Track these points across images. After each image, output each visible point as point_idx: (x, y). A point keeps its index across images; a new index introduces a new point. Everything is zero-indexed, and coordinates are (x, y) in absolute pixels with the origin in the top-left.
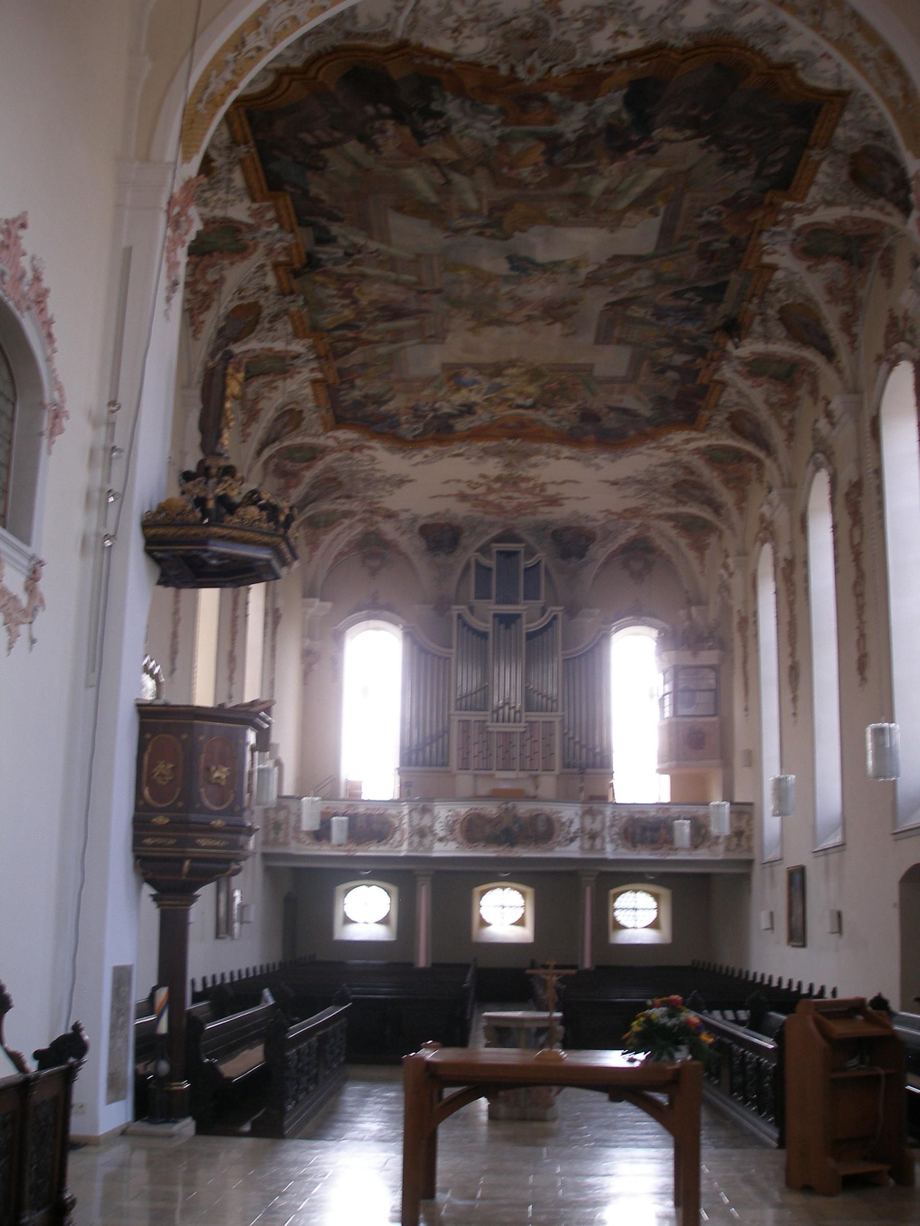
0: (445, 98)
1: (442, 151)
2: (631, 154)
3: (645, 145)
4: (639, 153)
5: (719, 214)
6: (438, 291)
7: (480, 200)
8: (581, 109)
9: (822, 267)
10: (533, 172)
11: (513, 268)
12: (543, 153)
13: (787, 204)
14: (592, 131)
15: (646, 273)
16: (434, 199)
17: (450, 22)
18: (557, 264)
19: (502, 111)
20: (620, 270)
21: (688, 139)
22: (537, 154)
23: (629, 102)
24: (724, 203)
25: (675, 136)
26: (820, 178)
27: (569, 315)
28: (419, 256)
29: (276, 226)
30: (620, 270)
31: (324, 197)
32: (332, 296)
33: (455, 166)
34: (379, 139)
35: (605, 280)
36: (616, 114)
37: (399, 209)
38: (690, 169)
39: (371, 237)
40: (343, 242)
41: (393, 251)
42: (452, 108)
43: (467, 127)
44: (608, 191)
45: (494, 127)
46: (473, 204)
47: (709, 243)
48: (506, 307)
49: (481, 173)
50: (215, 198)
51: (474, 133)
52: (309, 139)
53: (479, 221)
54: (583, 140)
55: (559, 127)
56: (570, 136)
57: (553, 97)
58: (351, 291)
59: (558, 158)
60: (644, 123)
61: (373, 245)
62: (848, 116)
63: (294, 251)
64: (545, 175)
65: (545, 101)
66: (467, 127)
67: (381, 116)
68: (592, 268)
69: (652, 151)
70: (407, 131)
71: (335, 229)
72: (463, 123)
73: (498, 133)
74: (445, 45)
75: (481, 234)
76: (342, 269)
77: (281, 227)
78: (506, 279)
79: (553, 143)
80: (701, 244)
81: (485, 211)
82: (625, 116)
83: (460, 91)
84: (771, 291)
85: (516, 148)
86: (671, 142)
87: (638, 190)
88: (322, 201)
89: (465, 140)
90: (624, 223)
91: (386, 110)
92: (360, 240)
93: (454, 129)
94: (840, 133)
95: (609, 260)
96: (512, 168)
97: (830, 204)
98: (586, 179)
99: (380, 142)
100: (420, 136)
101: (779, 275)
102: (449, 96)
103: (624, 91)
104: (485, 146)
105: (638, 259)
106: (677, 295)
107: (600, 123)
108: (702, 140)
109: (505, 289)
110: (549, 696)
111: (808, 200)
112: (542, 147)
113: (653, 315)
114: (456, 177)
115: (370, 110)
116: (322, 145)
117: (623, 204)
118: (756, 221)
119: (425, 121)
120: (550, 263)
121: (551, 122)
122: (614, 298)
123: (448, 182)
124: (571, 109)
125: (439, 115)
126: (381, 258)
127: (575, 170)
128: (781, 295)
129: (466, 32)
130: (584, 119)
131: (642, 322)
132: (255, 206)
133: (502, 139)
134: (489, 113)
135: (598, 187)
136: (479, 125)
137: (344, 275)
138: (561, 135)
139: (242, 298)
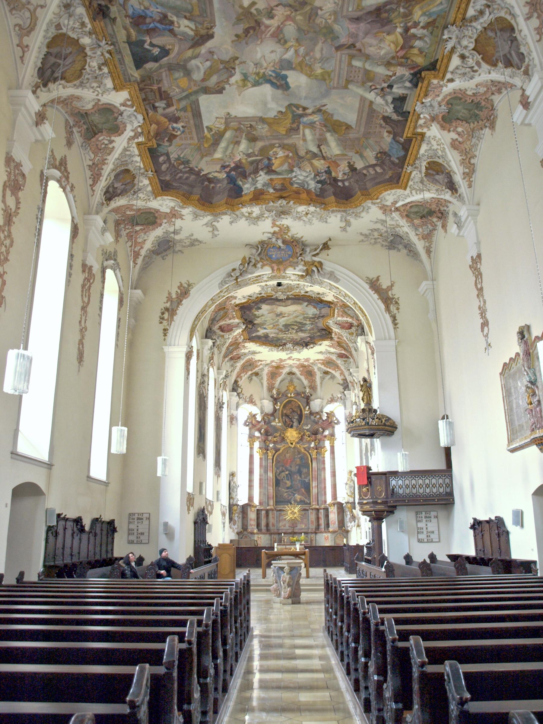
0: (315, 189)
1: (320, 164)
2: (233, 165)
3: (227, 170)
4: (229, 166)
5: (174, 129)
6: (338, 48)
7: (304, 135)
8: (259, 186)
9: (93, 103)
10: (277, 154)
11: (285, 77)
12: (273, 164)
13: (141, 139)
14: (252, 176)
15: (197, 76)
16: (328, 135)
17: (309, 216)
18: (256, 84)
19: (292, 184)
20: (214, 80)
21: (209, 173)
22: (276, 164)
23: (240, 189)
24: (175, 136)
25: (216, 174)
26: (138, 159)
27: (239, 20)
28: (346, 87)
29: (422, 116)
30: (214, 80)
31: (386, 134)
32: (420, 38)
33: (315, 156)
34: (347, 170)
35: (221, 67)
36: (244, 184)
37: (348, 127)
38: (202, 158)
39: (371, 103)
40: (390, 99)
41: (360, 91)
42: (312, 185)
43: (307, 177)
44: (238, 143)
45: (295, 177)
46: (307, 132)
47: (169, 105)
48: (290, 30)
49: (302, 153)
50: (439, 147)
51: (304, 174)
52: (378, 169)
53: (305, 119)
54: (256, 171)
55: (268, 177)
56: (261, 173)
57: (271, 191)
58: (402, 48)
59: (266, 161)
60: (231, 180)
61: (371, 96)
62: (149, 188)
63: (422, 95)
64: (271, 152)
65: (274, 189)
66: (307, 177)
67: (343, 181)
68: (233, 80)
69: (223, 167)
70: (333, 174)
71: (389, 110)
72: (309, 178)
73: (294, 174)
74: (312, 209)
75: (305, 109)
76: (401, 71)
77: (419, 115)
78: (289, 65)
79: (269, 170)
80: (173, 105)
81: (301, 127)
82: (240, 183)
83: (309, 192)
84: (103, 64)
85: (285, 167)
86: (216, 172)
87: (223, 144)
88: (387, 132)
89: (308, 170)
90: (223, 121)
91: (340, 184)
92: (379, 100)
93: (313, 176)
94: (146, 182)
95: (224, 89)
96: (287, 156)
97: (125, 150)
98: (251, 151)
99: (347, 168)
100: (328, 172)
101: (109, 83)
102: (313, 191)
103: (243, 193)
104: (300, 168)
105: (206, 91)
106: (165, 52)
107: (250, 180)
108: (203, 173)
109: (290, 55)
110: (256, 322)
111: (134, 145)
112: (273, 168)
113: (172, 23)
114: (315, 150)
115: (347, 184)
116: (373, 166)
117: (228, 134)
118: (151, 125)
119: (325, 179)
120: (261, 84)
121: (271, 180)
122: (209, 44)
123: (319, 146)
124: (264, 186)
125: (318, 182)
126: (370, 84)
127: (257, 156)
128: (94, 64)
129: (304, 213)
130: (257, 181)
131: (178, 11)
132: (425, 130)
133: (292, 171)
134: (297, 183)
135: (244, 145)
136: (301, 178)
137: (401, 65)
138: (266, 173)
139: (478, 64)
